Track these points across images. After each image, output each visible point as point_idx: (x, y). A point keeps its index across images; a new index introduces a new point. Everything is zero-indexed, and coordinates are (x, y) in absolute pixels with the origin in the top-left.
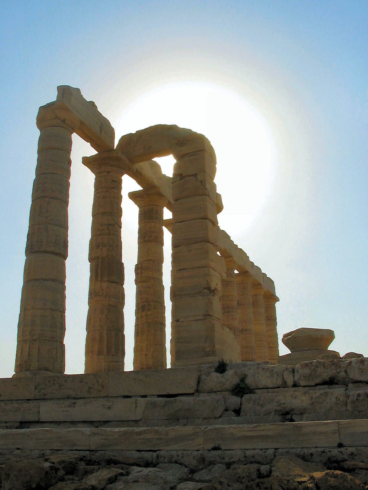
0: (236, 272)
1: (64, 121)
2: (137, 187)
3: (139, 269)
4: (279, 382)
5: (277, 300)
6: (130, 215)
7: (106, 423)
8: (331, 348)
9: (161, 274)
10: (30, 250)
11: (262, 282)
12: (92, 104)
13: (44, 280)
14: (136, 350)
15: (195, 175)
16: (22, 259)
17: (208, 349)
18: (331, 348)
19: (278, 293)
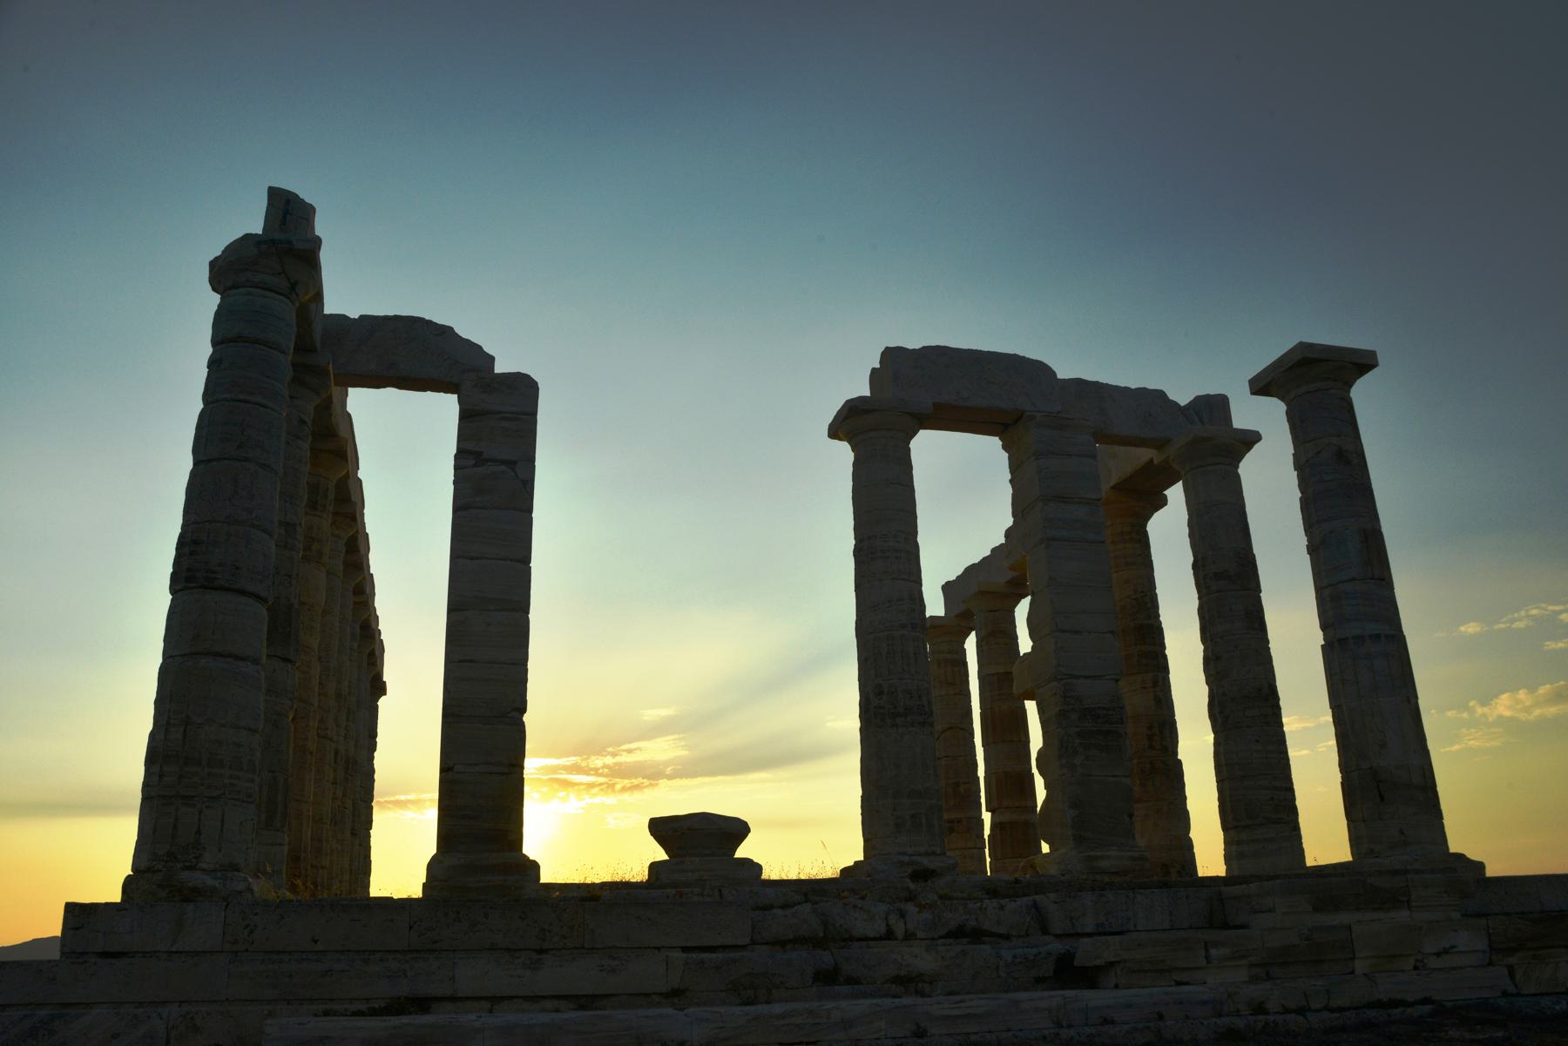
1: (293, 287)
8: (741, 852)
13: (237, 658)
15: (511, 464)
18: (741, 852)
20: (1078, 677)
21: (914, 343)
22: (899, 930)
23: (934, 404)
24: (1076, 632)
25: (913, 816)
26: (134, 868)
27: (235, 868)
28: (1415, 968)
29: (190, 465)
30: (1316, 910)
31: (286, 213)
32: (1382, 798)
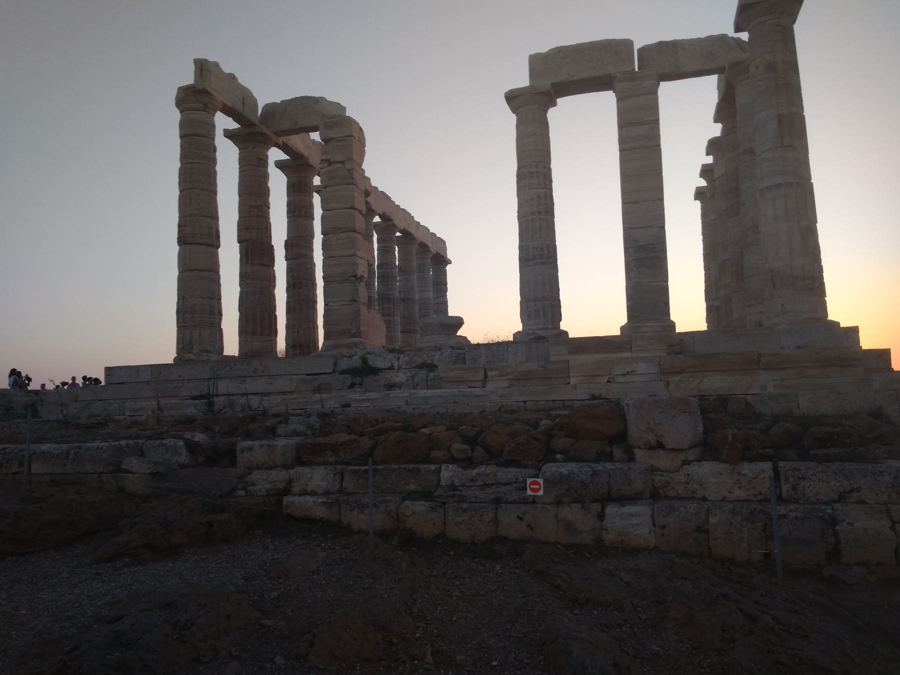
0: (398, 234)
1: (206, 105)
2: (283, 156)
3: (288, 245)
4: (389, 365)
5: (449, 262)
6: (278, 185)
7: (268, 394)
8: (461, 332)
9: (311, 250)
10: (182, 240)
11: (430, 245)
12: (232, 77)
13: (200, 270)
14: (288, 327)
15: (342, 162)
16: (174, 249)
17: (353, 332)
18: (460, 333)
19: (449, 257)
20: (634, 228)
21: (544, 49)
22: (396, 366)
23: (552, 84)
24: (637, 202)
25: (536, 311)
26: (178, 353)
27: (209, 352)
28: (608, 382)
29: (178, 193)
30: (570, 353)
31: (202, 70)
32: (774, 285)
